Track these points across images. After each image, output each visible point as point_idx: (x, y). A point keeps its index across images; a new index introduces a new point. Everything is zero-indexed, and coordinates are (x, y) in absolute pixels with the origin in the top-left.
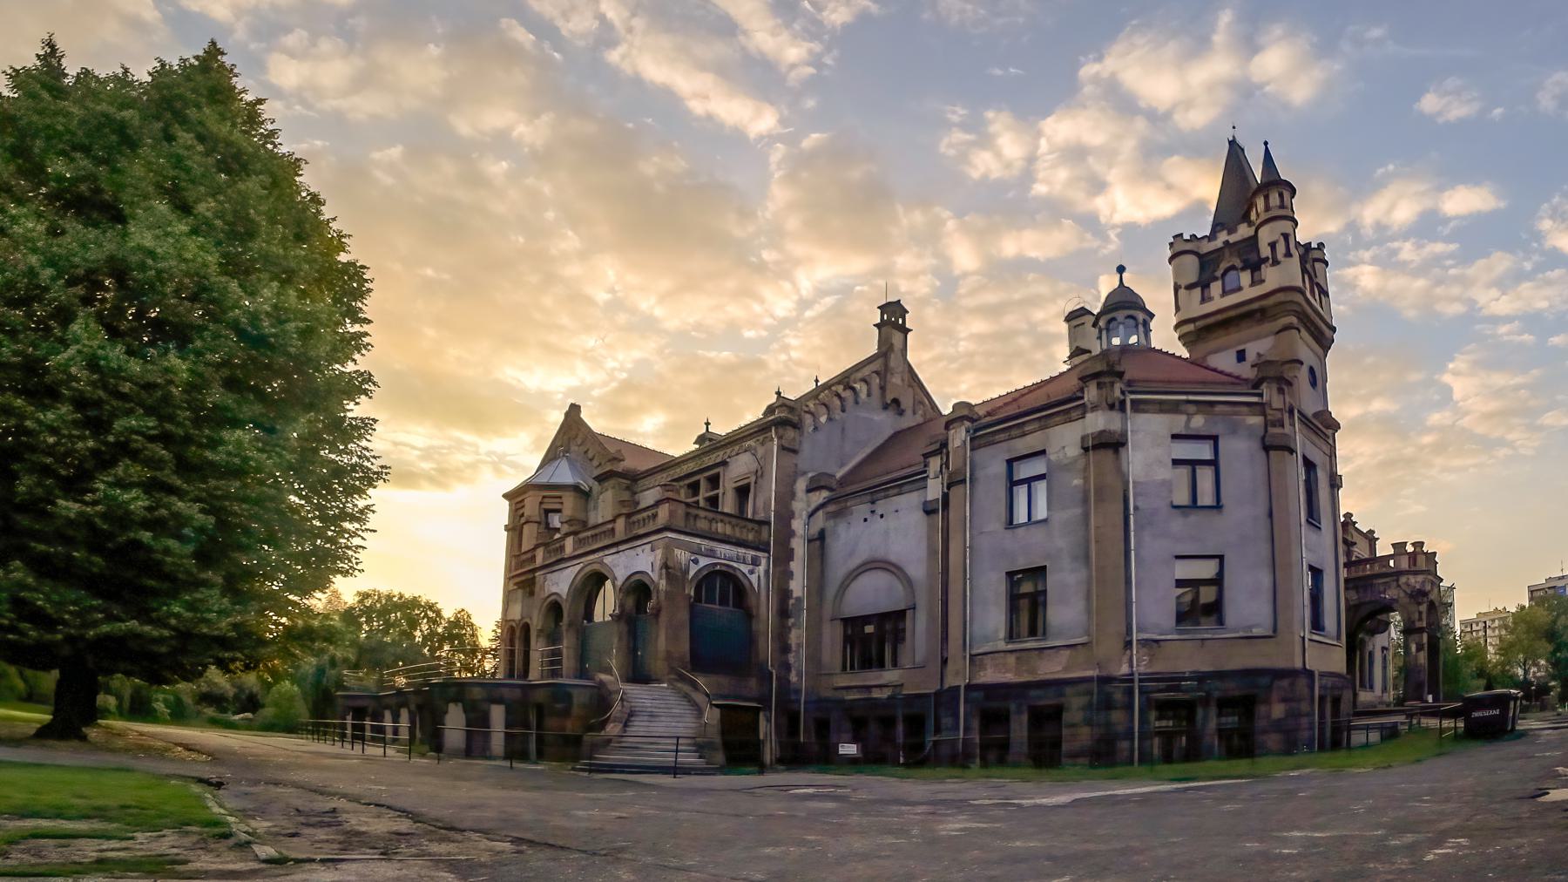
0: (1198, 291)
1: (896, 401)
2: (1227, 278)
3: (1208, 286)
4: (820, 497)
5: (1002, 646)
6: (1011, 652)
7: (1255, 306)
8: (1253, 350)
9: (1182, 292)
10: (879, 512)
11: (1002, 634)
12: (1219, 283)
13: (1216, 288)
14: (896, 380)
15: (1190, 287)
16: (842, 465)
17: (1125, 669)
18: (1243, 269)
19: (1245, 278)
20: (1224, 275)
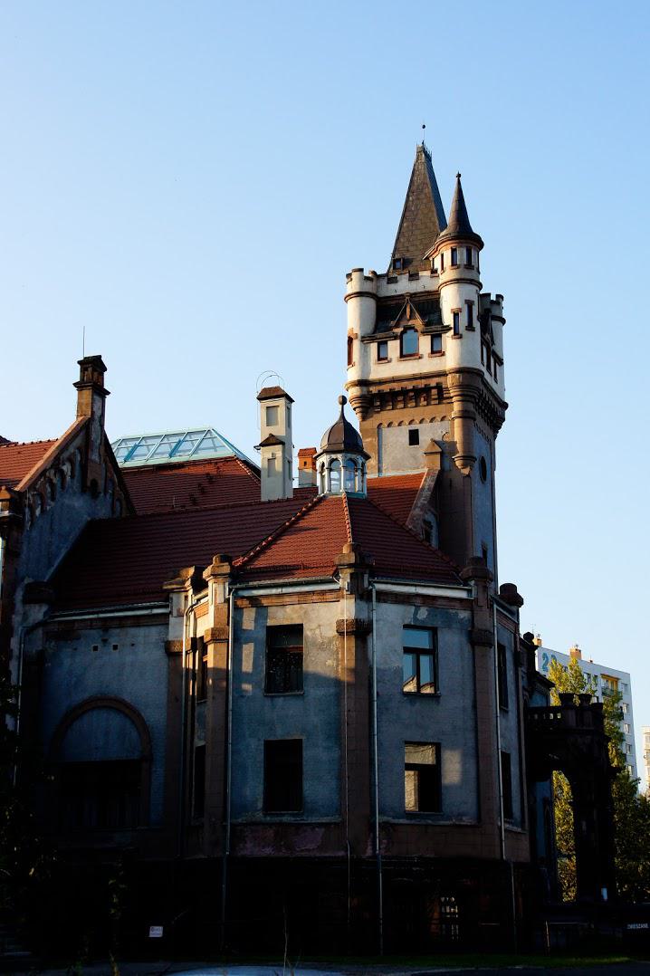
0: (374, 347)
1: (94, 482)
2: (404, 336)
3: (386, 343)
4: (38, 613)
5: (260, 816)
6: (270, 825)
7: (433, 382)
8: (428, 434)
9: (356, 344)
10: (113, 641)
11: (260, 805)
12: (398, 341)
13: (393, 347)
14: (95, 457)
15: (366, 339)
16: (50, 565)
17: (369, 852)
18: (424, 333)
19: (424, 343)
20: (402, 333)
